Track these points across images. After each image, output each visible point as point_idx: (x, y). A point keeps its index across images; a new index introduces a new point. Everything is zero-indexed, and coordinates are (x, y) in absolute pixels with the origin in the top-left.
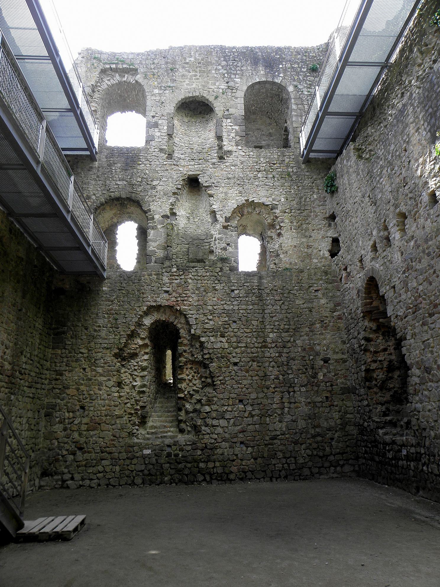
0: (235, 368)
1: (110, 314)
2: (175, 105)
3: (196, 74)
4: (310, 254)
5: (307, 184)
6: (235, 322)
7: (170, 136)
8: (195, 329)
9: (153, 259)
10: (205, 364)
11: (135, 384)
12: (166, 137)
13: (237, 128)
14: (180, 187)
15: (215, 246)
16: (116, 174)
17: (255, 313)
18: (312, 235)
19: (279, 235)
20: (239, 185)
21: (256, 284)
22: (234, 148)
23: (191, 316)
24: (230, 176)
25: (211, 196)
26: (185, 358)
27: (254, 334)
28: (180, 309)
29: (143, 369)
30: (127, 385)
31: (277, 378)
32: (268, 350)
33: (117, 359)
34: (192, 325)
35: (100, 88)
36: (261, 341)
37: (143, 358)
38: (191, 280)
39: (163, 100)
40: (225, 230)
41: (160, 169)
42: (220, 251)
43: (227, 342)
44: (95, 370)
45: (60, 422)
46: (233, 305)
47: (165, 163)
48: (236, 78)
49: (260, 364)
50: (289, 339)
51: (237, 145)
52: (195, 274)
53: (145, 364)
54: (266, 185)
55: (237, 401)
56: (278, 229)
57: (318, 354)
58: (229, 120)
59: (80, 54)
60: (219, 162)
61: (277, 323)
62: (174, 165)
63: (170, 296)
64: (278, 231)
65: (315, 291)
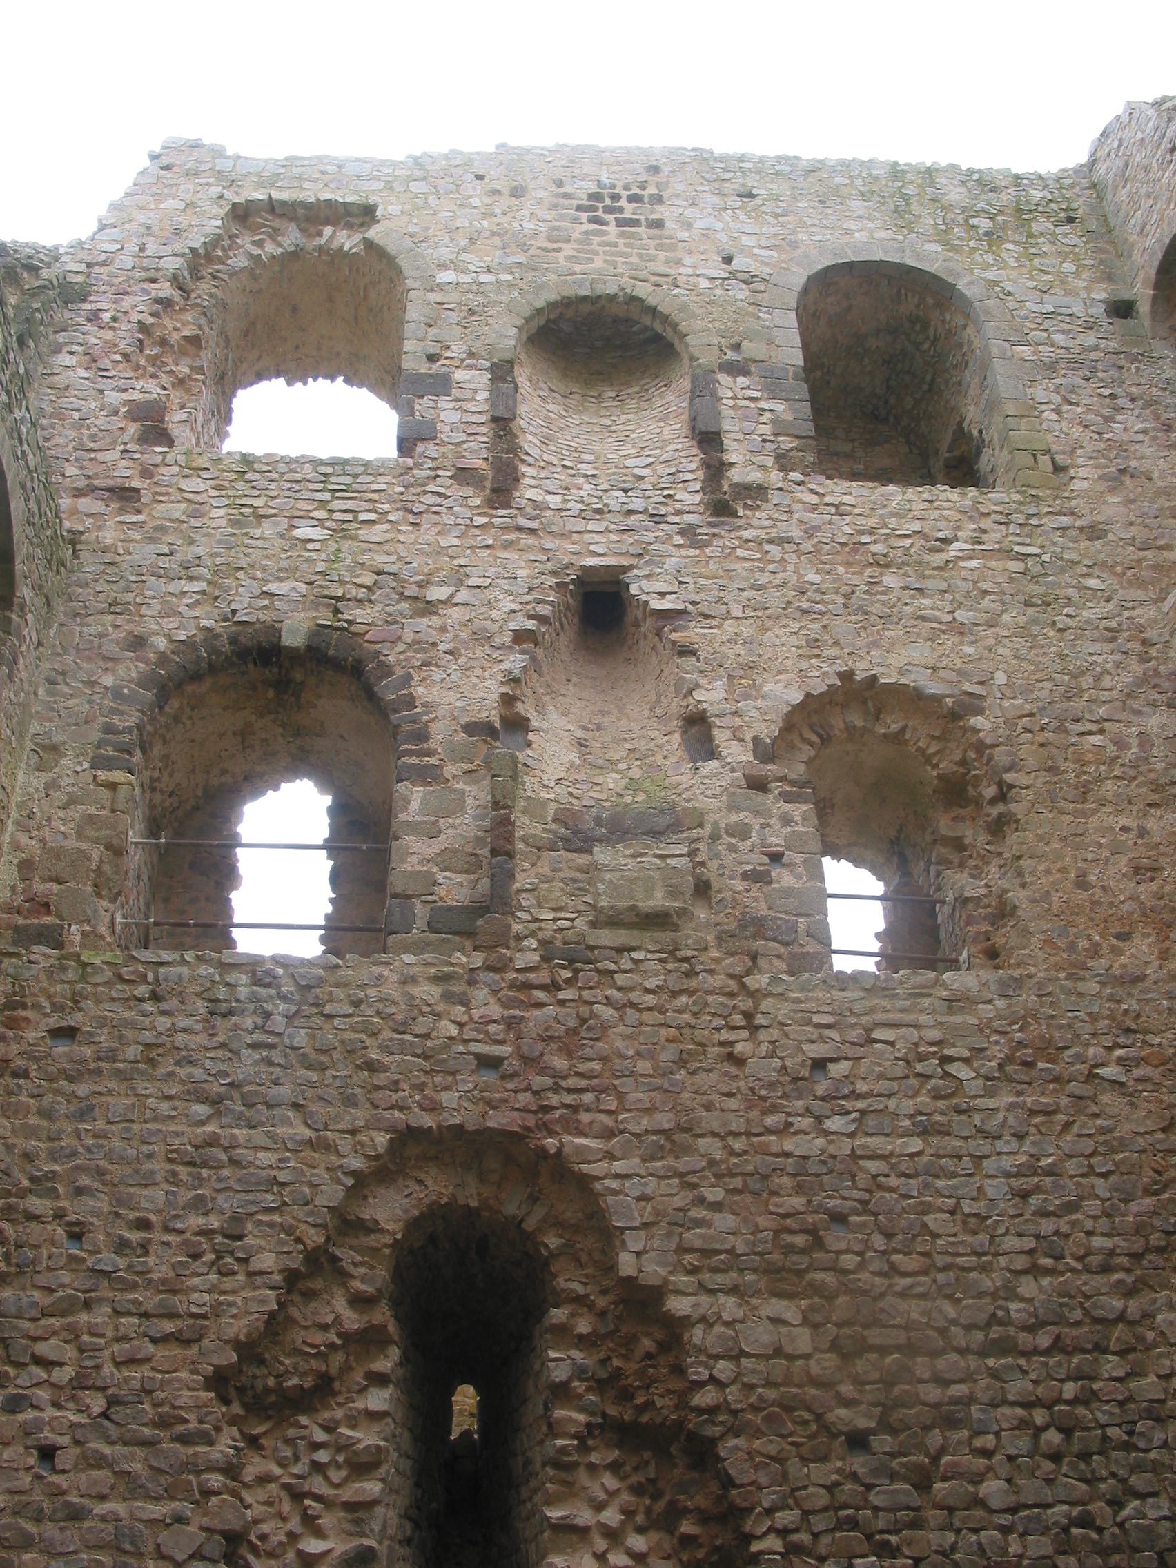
0: (859, 1463)
2: (519, 322)
6: (839, 1218)
7: (502, 424)
8: (638, 1254)
9: (420, 911)
10: (692, 1437)
11: (313, 1546)
12: (484, 429)
13: (779, 406)
14: (545, 610)
17: (937, 1177)
19: (998, 828)
20: (804, 612)
22: (775, 478)
23: (614, 1184)
24: (763, 578)
25: (686, 651)
26: (582, 1410)
27: (941, 1277)
28: (559, 1151)
29: (362, 1466)
30: (271, 1555)
32: (1022, 1361)
33: (226, 1401)
34: (622, 1230)
35: (220, 267)
36: (983, 1317)
37: (360, 1405)
38: (611, 1011)
40: (759, 797)
41: (456, 542)
42: (739, 885)
43: (805, 1321)
46: (826, 1133)
49: (988, 1441)
50: (1118, 1304)
51: (784, 469)
53: (366, 1438)
54: (923, 618)
56: (993, 802)
59: (154, 157)
60: (710, 524)
62: (519, 529)
63: (510, 1086)
64: (995, 811)
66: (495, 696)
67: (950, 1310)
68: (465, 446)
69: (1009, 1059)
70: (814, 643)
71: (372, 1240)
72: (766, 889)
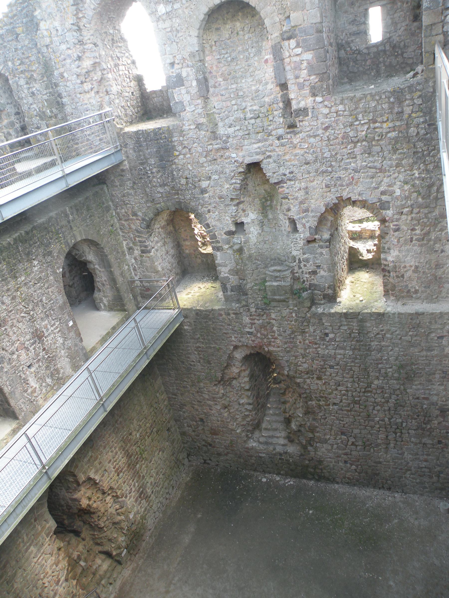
0: (336, 407)
4: (439, 278)
15: (301, 270)
16: (154, 177)
24: (310, 157)
31: (383, 420)
42: (307, 276)
44: (202, 396)
47: (210, 147)
51: (314, 95)
54: (370, 168)
58: (293, 42)
60: (288, 133)
65: (438, 338)
66: (230, 222)
68: (196, 112)
70: (327, 186)
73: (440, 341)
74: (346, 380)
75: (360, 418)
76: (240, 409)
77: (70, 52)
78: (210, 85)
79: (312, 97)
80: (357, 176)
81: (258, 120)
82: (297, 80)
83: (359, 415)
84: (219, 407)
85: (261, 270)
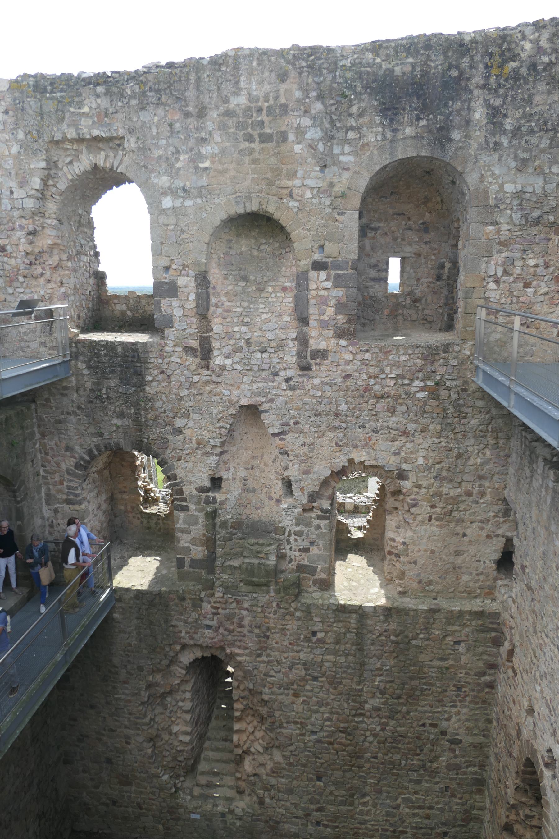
1: (129, 651)
3: (252, 145)
5: (475, 428)
13: (340, 293)
16: (110, 403)
18: (468, 532)
21: (354, 626)
24: (321, 408)
39: (182, 225)
42: (297, 554)
45: (84, 771)
46: (314, 654)
47: (196, 379)
48: (343, 154)
52: (254, 602)
55: (315, 778)
57: (444, 733)
58: (323, 275)
61: (382, 685)
66: (206, 475)
67: (346, 705)
68: (187, 331)
69: (381, 635)
71: (181, 665)
72: (307, 554)
73: (456, 647)
74: (332, 697)
75: (345, 753)
76: (170, 741)
77: (24, 221)
78: (211, 302)
79: (335, 338)
80: (375, 436)
81: (265, 355)
82: (322, 317)
83: (344, 750)
84: (140, 739)
85: (237, 541)
